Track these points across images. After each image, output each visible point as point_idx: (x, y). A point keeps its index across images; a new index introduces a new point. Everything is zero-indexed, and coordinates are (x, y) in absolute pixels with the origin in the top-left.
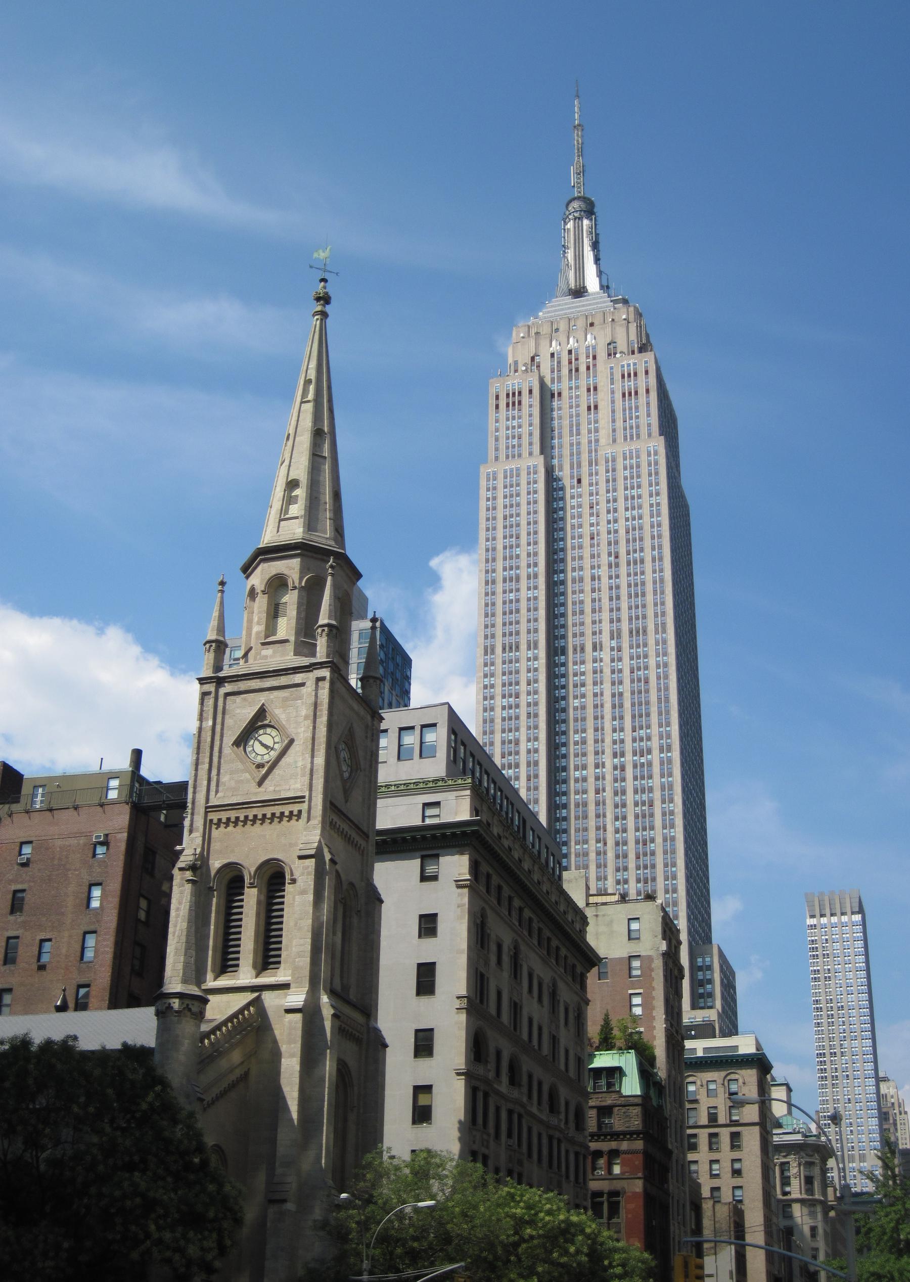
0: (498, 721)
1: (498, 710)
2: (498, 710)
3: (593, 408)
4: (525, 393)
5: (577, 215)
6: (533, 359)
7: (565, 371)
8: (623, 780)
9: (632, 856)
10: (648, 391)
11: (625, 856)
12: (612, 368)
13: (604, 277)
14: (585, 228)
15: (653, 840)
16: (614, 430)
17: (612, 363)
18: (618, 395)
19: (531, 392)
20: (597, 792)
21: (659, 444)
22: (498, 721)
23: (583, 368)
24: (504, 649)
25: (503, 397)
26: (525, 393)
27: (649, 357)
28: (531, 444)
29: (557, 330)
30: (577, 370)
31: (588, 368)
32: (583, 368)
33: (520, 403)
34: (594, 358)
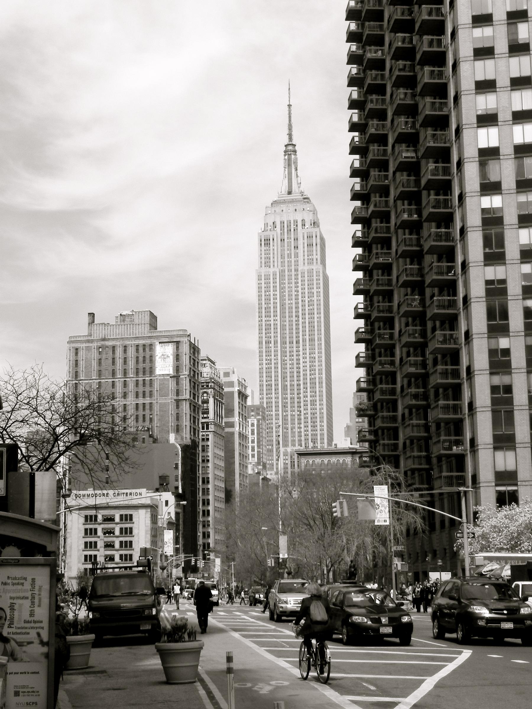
0: (264, 369)
1: (264, 365)
2: (264, 365)
3: (296, 247)
4: (271, 240)
5: (289, 153)
6: (274, 223)
7: (286, 230)
8: (307, 392)
9: (309, 418)
10: (316, 245)
11: (307, 418)
12: (303, 233)
13: (299, 178)
14: (292, 160)
15: (316, 413)
16: (304, 260)
17: (304, 231)
18: (306, 245)
19: (273, 239)
20: (298, 394)
21: (320, 267)
22: (264, 369)
23: (292, 230)
24: (266, 343)
25: (263, 240)
26: (271, 240)
27: (317, 230)
28: (274, 262)
29: (283, 211)
30: (290, 230)
31: (294, 230)
32: (292, 230)
33: (269, 244)
34: (297, 226)
